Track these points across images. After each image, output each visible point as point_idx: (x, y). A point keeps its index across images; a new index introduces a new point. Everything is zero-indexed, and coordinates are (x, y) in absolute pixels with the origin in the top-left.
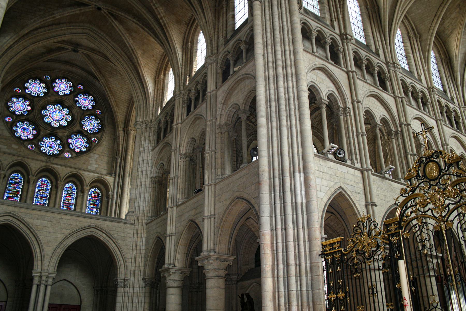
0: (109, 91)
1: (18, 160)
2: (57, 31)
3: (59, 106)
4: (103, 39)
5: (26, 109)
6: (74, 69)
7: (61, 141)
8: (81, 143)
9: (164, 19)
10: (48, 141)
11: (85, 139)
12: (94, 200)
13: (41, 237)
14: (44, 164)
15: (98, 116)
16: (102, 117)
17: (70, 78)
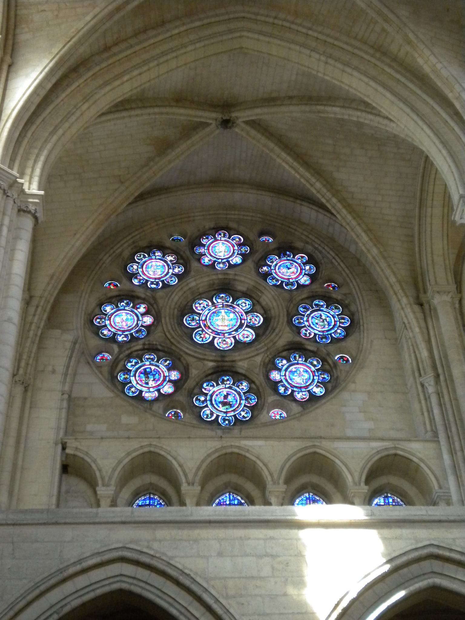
0: (344, 207)
1: (142, 447)
5: (140, 323)
7: (251, 382)
8: (306, 376)
11: (315, 363)
15: (334, 296)
16: (345, 295)
17: (232, 225)
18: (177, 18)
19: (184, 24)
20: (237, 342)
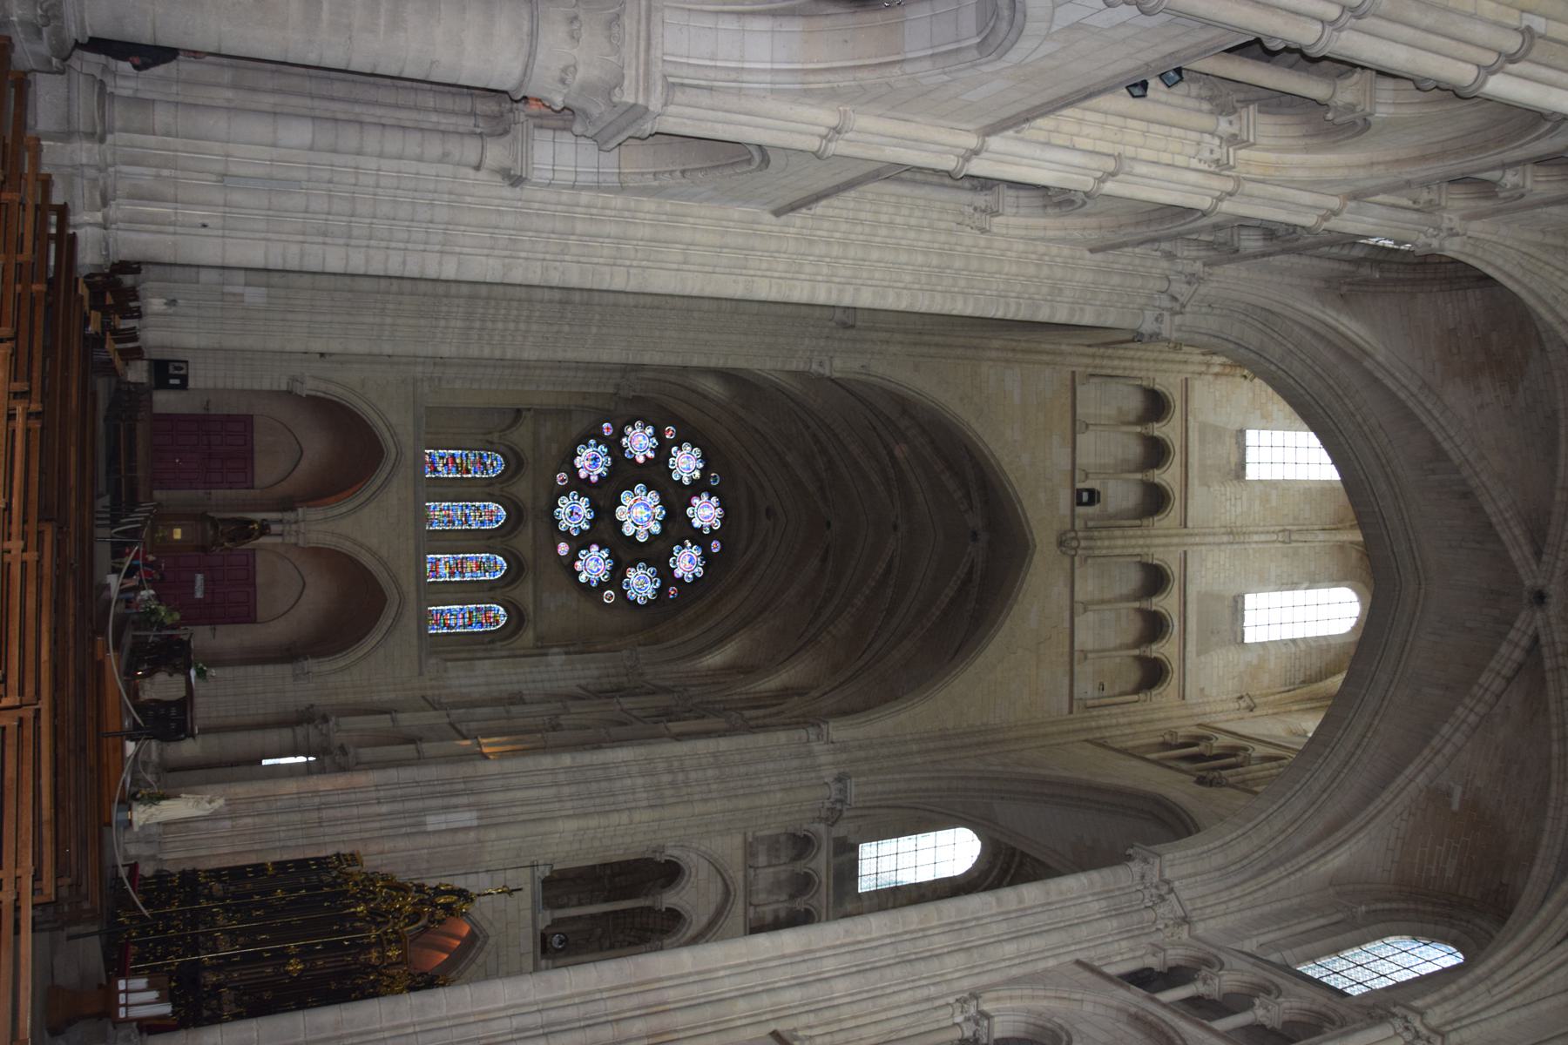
3: (661, 512)
7: (589, 531)
10: (583, 506)
12: (481, 617)
20: (622, 523)
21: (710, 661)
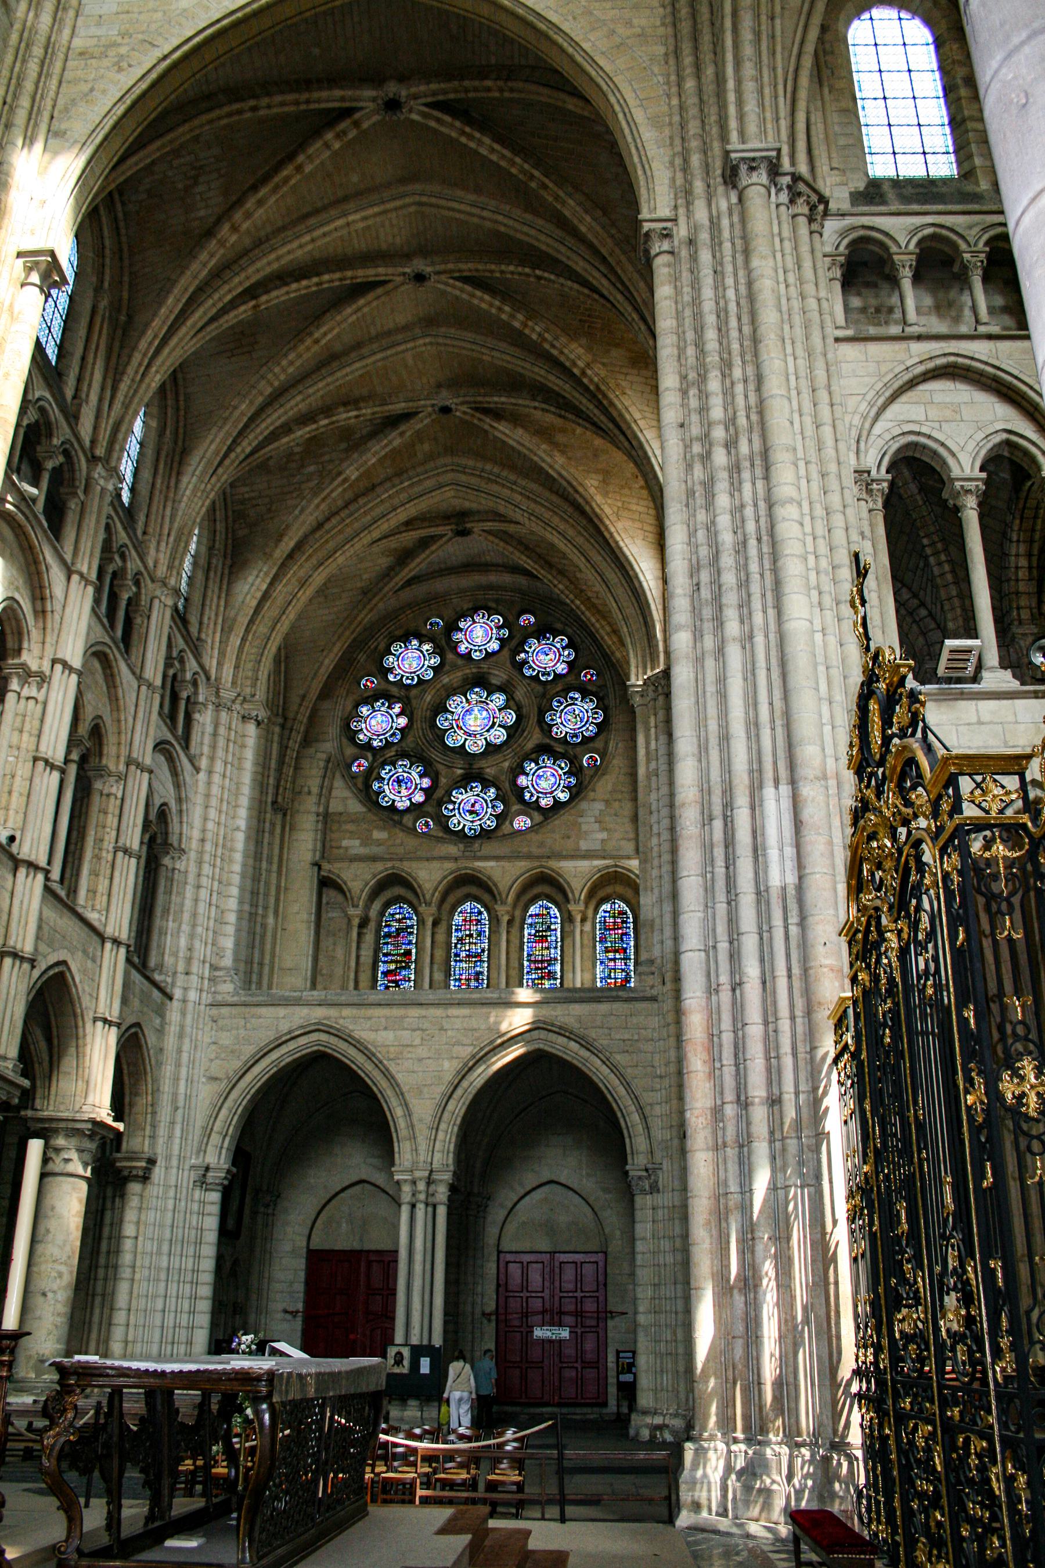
0: (588, 609)
1: (386, 869)
2: (371, 509)
4: (497, 483)
6: (493, 578)
7: (498, 789)
8: (553, 780)
9: (589, 372)
10: (463, 797)
12: (612, 936)
13: (400, 1077)
14: (450, 866)
17: (493, 605)
18: (389, 479)
19: (394, 486)
20: (488, 744)
21: (649, 576)
